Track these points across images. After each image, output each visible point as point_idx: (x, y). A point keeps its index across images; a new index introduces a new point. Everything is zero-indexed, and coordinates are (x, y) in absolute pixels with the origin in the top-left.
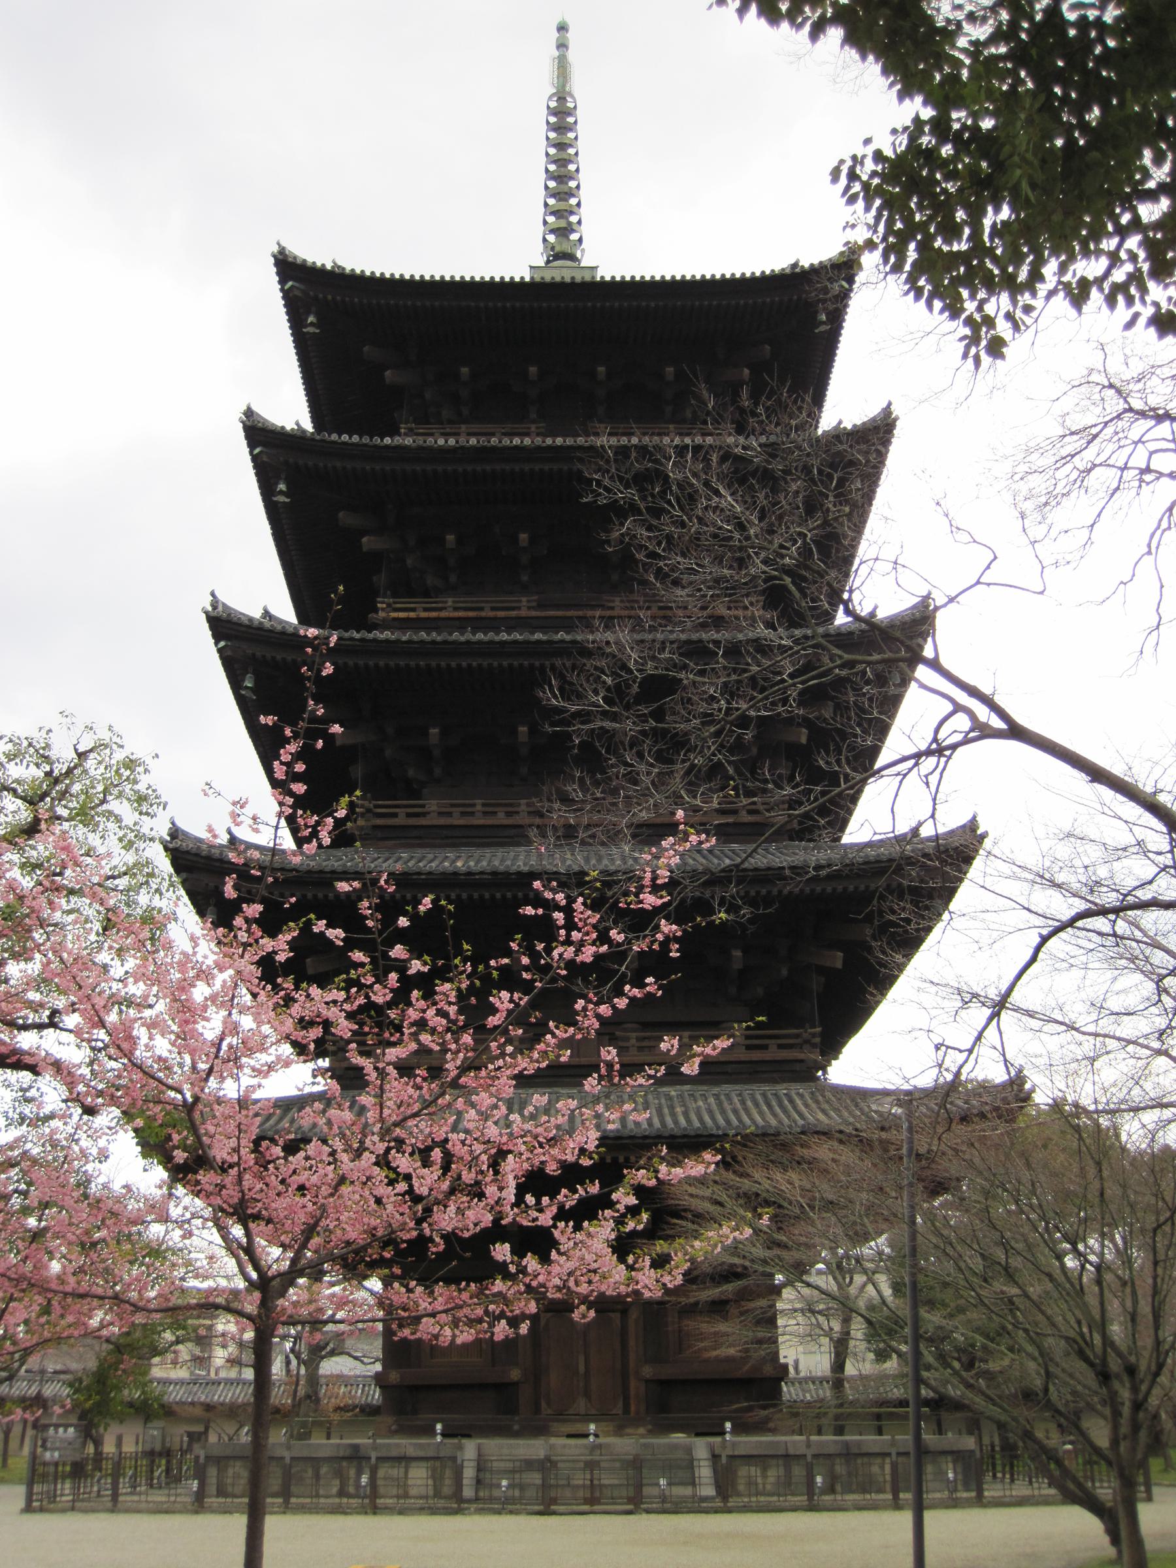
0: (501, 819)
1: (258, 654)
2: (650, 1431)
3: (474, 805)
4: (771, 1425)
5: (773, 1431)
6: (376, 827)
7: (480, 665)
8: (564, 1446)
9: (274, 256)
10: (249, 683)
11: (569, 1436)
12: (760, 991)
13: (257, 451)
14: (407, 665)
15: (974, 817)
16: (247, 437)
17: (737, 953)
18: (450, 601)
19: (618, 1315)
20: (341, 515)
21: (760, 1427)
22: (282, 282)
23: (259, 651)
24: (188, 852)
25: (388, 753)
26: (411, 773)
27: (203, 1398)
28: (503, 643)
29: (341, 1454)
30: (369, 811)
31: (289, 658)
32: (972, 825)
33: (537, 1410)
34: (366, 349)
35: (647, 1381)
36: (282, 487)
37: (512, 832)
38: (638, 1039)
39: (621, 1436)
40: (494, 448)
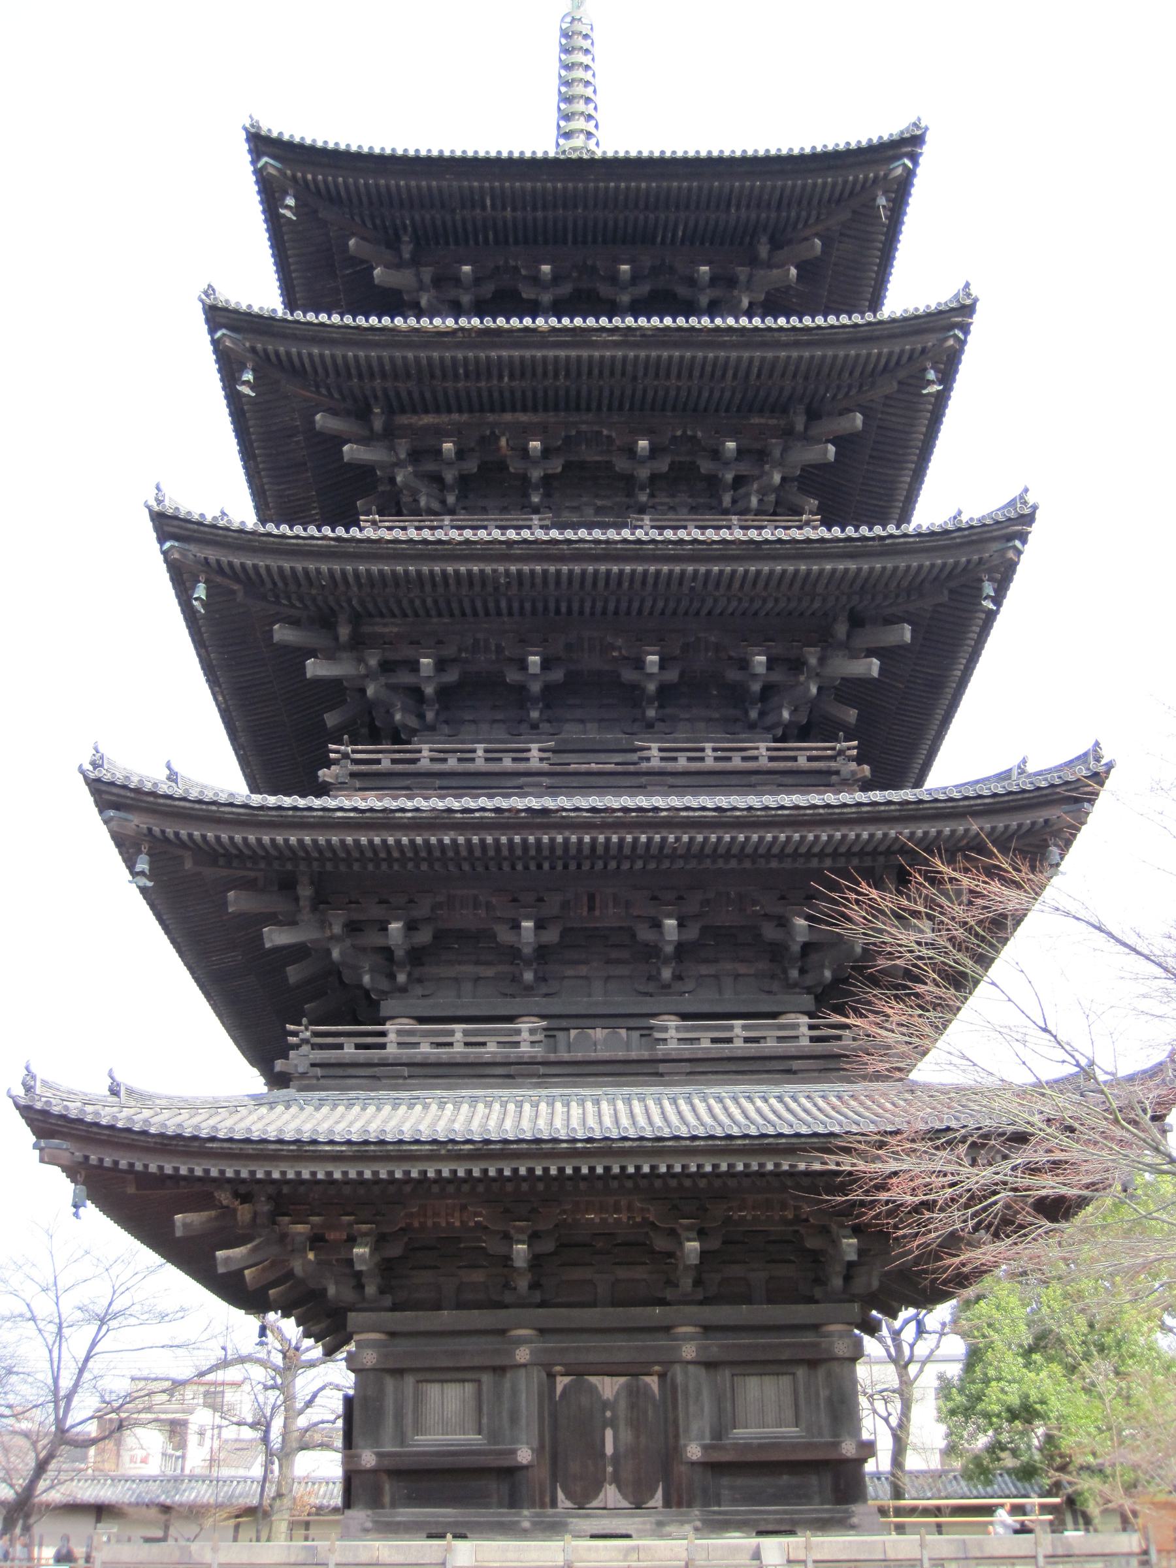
0: (507, 764)
1: (212, 558)
2: (696, 1529)
3: (474, 751)
4: (855, 1520)
5: (853, 1527)
6: (353, 775)
7: (482, 571)
8: (589, 1549)
9: (245, 129)
10: (201, 591)
11: (593, 1536)
12: (828, 974)
13: (219, 334)
14: (394, 572)
15: (1097, 744)
16: (208, 321)
17: (801, 922)
18: (447, 520)
19: (655, 1378)
20: (318, 417)
21: (841, 1523)
22: (254, 162)
23: (212, 554)
24: (112, 784)
25: (370, 691)
26: (398, 717)
27: (162, 1498)
28: (510, 543)
29: (292, 1560)
30: (346, 756)
31: (249, 563)
32: (1095, 752)
33: (554, 1504)
34: (352, 242)
35: (693, 1464)
36: (248, 376)
37: (523, 780)
38: (677, 1029)
39: (662, 1537)
40: (499, 331)
